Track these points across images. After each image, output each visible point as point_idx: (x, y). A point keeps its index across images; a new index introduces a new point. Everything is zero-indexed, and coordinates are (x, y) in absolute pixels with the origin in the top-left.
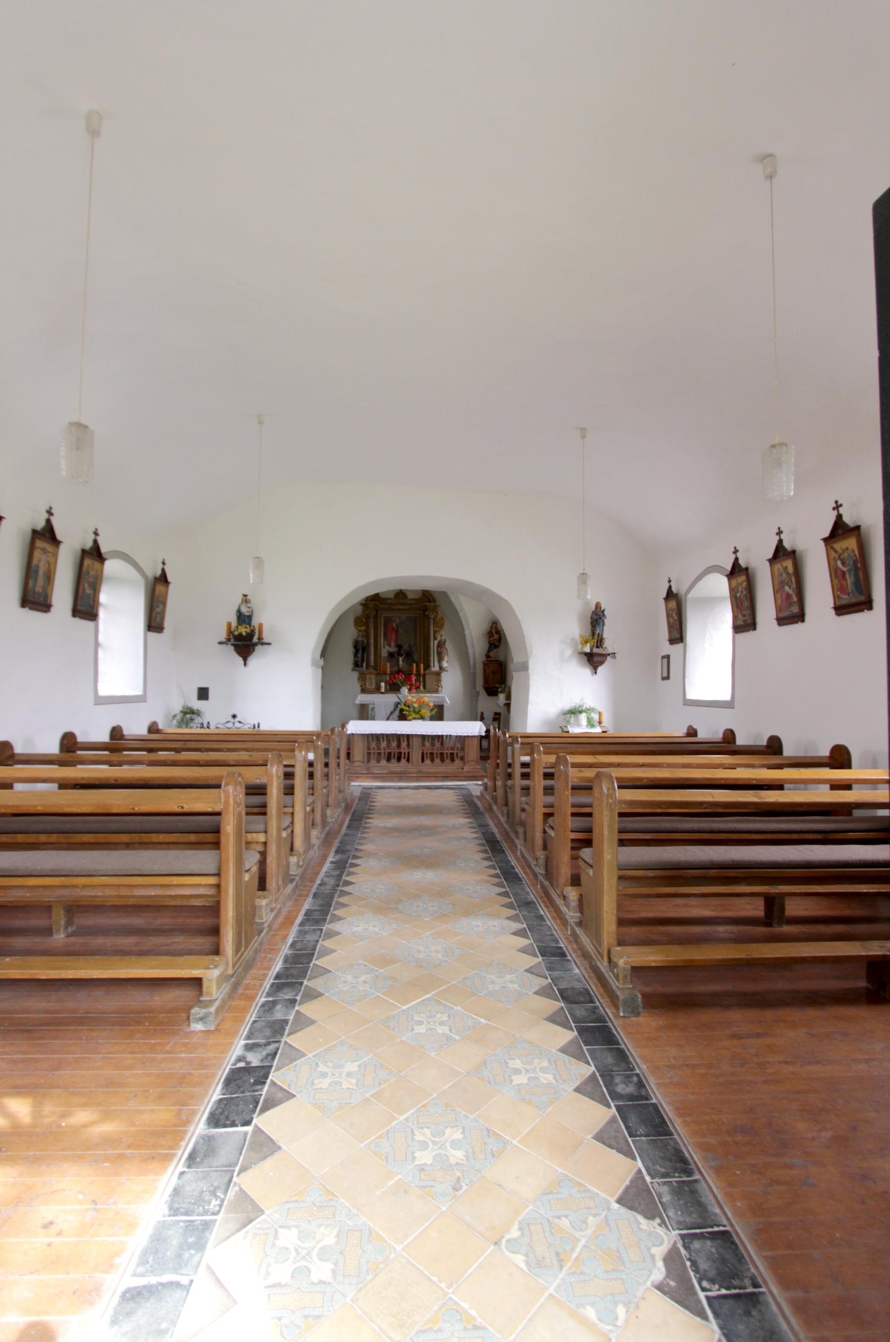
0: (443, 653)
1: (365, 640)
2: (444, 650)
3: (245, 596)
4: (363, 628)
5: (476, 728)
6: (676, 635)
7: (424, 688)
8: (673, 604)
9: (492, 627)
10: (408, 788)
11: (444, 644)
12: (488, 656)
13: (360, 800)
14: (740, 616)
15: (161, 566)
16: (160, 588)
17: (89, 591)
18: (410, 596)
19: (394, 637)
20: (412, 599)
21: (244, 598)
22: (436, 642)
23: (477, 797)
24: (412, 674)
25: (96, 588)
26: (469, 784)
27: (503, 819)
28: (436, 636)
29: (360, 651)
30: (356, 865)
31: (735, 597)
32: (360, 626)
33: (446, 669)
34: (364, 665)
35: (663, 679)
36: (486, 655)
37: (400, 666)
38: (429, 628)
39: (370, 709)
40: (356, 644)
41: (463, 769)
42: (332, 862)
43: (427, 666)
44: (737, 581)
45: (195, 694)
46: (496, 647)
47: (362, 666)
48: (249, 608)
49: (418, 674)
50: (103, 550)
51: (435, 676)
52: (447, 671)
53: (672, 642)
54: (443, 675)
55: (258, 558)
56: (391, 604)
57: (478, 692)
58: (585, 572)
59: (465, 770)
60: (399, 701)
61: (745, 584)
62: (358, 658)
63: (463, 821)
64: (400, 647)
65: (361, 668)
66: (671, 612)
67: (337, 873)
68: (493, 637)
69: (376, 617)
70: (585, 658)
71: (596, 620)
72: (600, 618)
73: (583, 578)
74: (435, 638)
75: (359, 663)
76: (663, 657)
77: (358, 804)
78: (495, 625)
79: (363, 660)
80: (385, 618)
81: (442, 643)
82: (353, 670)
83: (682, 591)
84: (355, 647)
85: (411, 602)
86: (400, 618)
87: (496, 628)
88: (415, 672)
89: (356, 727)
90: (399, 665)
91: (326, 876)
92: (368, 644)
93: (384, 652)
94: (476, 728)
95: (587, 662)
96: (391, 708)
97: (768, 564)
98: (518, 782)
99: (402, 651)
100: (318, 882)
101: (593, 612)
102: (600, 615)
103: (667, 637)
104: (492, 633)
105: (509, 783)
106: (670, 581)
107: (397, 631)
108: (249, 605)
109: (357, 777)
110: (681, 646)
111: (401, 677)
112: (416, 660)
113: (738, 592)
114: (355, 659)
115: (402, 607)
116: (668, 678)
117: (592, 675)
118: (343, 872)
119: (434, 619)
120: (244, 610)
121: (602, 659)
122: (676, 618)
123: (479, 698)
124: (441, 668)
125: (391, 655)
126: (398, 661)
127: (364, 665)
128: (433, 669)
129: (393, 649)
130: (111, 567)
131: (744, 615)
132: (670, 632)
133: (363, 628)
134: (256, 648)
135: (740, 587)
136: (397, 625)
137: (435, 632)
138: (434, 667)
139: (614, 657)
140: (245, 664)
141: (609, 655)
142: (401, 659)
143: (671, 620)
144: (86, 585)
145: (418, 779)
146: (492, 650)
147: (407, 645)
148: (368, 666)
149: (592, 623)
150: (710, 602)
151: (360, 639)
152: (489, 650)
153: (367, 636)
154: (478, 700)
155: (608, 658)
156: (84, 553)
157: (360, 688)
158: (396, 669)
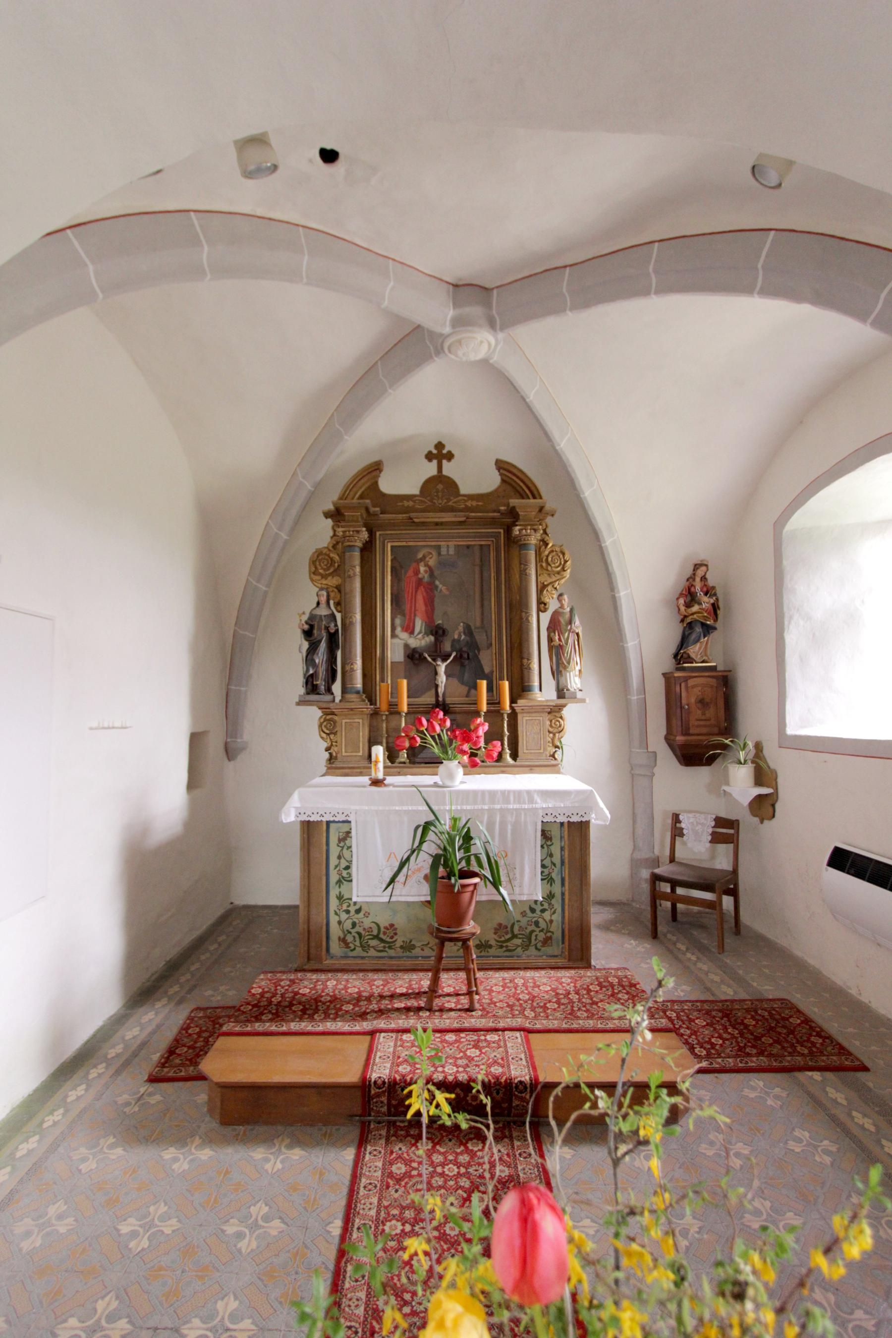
0: (569, 648)
1: (339, 616)
2: (572, 638)
4: (334, 581)
7: (515, 756)
9: (692, 578)
11: (570, 622)
12: (680, 657)
18: (463, 490)
19: (421, 604)
20: (471, 497)
22: (545, 618)
24: (477, 714)
28: (546, 600)
29: (323, 646)
32: (324, 577)
33: (579, 695)
34: (337, 688)
36: (675, 656)
37: (441, 690)
38: (524, 574)
40: (312, 627)
43: (520, 689)
46: (708, 629)
47: (329, 690)
49: (494, 713)
51: (545, 719)
52: (583, 701)
54: (570, 712)
56: (407, 510)
57: (655, 753)
60: (432, 818)
62: (314, 665)
64: (438, 632)
65: (328, 697)
68: (700, 604)
69: (368, 548)
74: (542, 606)
75: (321, 683)
79: (332, 675)
80: (392, 547)
81: (563, 620)
82: (301, 703)
84: (308, 634)
85: (469, 504)
86: (438, 548)
87: (704, 579)
88: (484, 707)
90: (437, 686)
92: (347, 626)
99: (447, 647)
107: (431, 588)
111: (442, 726)
112: (487, 670)
115: (448, 517)
119: (538, 553)
123: (656, 770)
125: (414, 657)
126: (436, 673)
129: (420, 640)
133: (334, 581)
137: (541, 589)
138: (541, 690)
142: (442, 667)
146: (697, 640)
147: (461, 627)
148: (344, 691)
151: (323, 611)
152: (684, 642)
154: (653, 775)
157: (327, 755)
158: (428, 699)
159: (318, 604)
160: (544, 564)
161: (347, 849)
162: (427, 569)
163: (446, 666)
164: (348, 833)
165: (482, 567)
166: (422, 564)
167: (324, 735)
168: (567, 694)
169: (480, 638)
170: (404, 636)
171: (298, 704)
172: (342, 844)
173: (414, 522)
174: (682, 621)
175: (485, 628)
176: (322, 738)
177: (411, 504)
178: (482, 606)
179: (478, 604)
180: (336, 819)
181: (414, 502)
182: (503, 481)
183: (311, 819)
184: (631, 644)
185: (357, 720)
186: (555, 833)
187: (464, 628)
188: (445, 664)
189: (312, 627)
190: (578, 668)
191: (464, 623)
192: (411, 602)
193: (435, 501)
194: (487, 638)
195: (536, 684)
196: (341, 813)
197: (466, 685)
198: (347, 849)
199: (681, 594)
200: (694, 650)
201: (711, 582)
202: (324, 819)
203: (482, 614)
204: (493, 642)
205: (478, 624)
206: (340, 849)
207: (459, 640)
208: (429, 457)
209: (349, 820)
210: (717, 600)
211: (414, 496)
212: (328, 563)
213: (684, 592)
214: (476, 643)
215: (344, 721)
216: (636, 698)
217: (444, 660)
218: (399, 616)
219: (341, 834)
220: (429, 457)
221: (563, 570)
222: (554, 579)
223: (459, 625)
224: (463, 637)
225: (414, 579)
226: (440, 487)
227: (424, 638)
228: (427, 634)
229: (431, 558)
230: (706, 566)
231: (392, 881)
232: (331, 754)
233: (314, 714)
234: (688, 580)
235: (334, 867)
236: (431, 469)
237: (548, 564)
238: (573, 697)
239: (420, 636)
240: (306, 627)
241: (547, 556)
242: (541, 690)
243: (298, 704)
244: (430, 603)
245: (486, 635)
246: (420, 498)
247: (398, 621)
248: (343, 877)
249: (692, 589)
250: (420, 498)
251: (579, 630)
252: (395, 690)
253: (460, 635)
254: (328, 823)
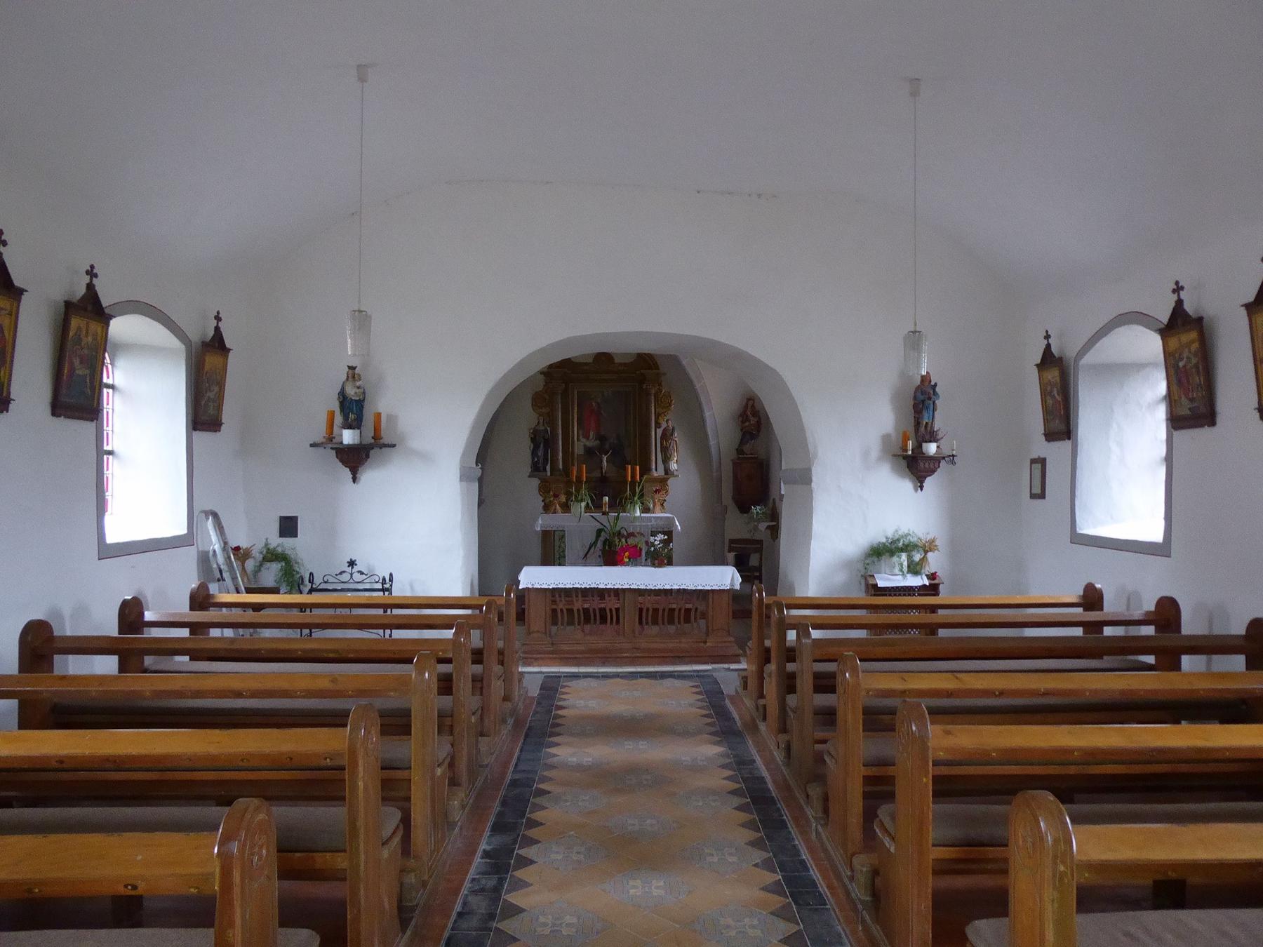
1: (549, 429)
3: (352, 368)
5: (724, 577)
6: (1058, 425)
8: (1053, 375)
9: (747, 404)
10: (617, 675)
12: (740, 451)
13: (539, 703)
14: (1184, 401)
15: (214, 323)
16: (211, 360)
17: (81, 371)
18: (617, 360)
20: (621, 364)
21: (351, 372)
22: (660, 431)
23: (732, 698)
25: (95, 366)
26: (714, 670)
27: (779, 756)
30: (527, 862)
31: (1176, 367)
33: (676, 473)
34: (548, 468)
35: (1033, 496)
38: (648, 410)
39: (557, 538)
40: (535, 436)
41: (705, 642)
42: (486, 854)
43: (646, 469)
44: (1180, 340)
45: (275, 527)
47: (545, 470)
48: (359, 388)
50: (105, 302)
53: (1050, 436)
55: (360, 311)
58: (918, 330)
59: (708, 644)
60: (602, 527)
61: (1195, 346)
63: (710, 750)
64: (602, 439)
65: (544, 473)
66: (1049, 388)
67: (491, 882)
68: (749, 421)
70: (904, 463)
71: (923, 401)
72: (930, 398)
73: (914, 339)
74: (658, 425)
76: (1033, 461)
77: (536, 713)
78: (750, 403)
83: (1070, 353)
84: (533, 440)
87: (753, 406)
89: (534, 577)
90: (602, 468)
91: (474, 892)
93: (579, 449)
94: (724, 577)
95: (907, 470)
96: (592, 538)
97: (1243, 312)
98: (807, 699)
99: (607, 446)
100: (458, 908)
101: (918, 388)
102: (929, 393)
103: (1040, 428)
104: (747, 416)
105: (792, 700)
106: (1047, 337)
108: (358, 384)
109: (536, 659)
110: (1065, 445)
113: (1181, 359)
114: (533, 459)
116: (1042, 495)
117: (916, 490)
118: (501, 881)
120: (351, 391)
121: (932, 466)
122: (1059, 398)
124: (667, 471)
125: (589, 452)
126: (602, 461)
127: (548, 468)
128: (655, 474)
130: (119, 327)
131: (1192, 400)
132: (1046, 421)
134: (372, 452)
135: (1187, 350)
138: (656, 470)
139: (953, 463)
140: (354, 480)
141: (944, 458)
143: (1050, 402)
144: (77, 362)
145: (633, 661)
148: (552, 469)
149: (915, 406)
150: (1122, 371)
151: (542, 428)
152: (742, 442)
153: (552, 422)
154: (725, 519)
155: (943, 463)
156: (69, 308)
157: (543, 504)
158: (597, 474)
159: (538, 423)
160: (660, 402)
164: (563, 536)
168: (669, 473)
170: (584, 440)
171: (529, 476)
174: (742, 430)
184: (712, 442)
189: (535, 436)
190: (675, 459)
195: (654, 467)
199: (741, 415)
200: (747, 448)
210: (760, 418)
211: (590, 363)
221: (670, 405)
222: (665, 410)
228: (596, 440)
230: (754, 400)
231: (586, 555)
232: (545, 504)
233: (535, 482)
237: (661, 402)
238: (672, 474)
241: (662, 398)
242: (656, 470)
243: (529, 476)
247: (581, 432)
251: (677, 439)
252: (579, 471)
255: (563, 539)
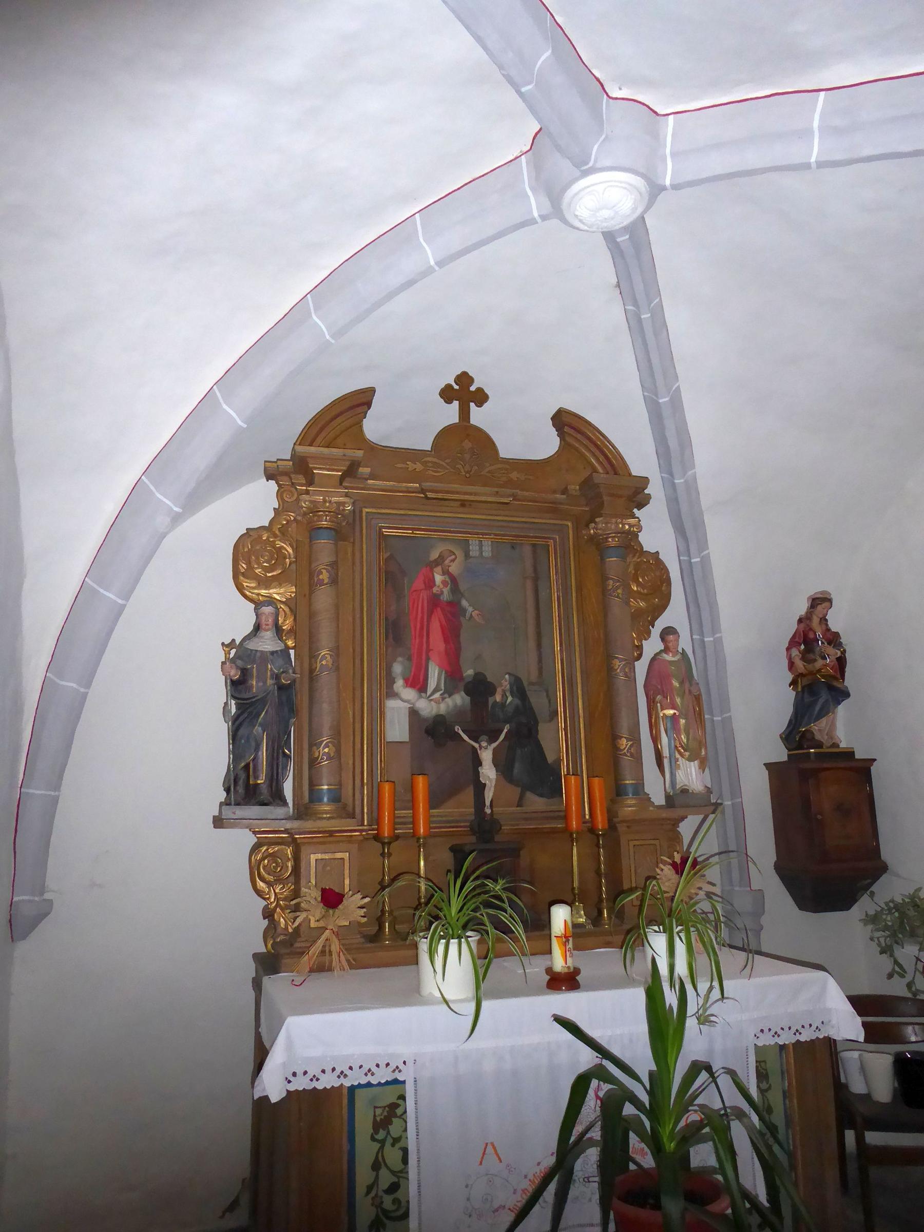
19: (437, 642)
32: (265, 583)
37: (489, 795)
40: (245, 672)
47: (277, 797)
56: (414, 477)
84: (237, 686)
85: (514, 475)
87: (824, 620)
90: (480, 788)
107: (453, 611)
126: (478, 763)
136: (453, 581)
142: (486, 756)
147: (506, 683)
151: (267, 643)
159: (257, 628)
161: (393, 1145)
162: (447, 579)
163: (494, 749)
165: (536, 580)
166: (438, 569)
167: (261, 885)
169: (537, 701)
170: (409, 694)
171: (218, 822)
172: (381, 1135)
173: (427, 498)
175: (545, 684)
176: (259, 893)
177: (419, 467)
178: (539, 645)
179: (532, 644)
180: (374, 1081)
181: (425, 464)
182: (565, 445)
183: (320, 1086)
185: (339, 855)
186: (773, 1065)
187: (510, 684)
188: (494, 745)
191: (510, 674)
192: (421, 636)
193: (459, 466)
194: (550, 701)
196: (382, 1065)
197: (517, 785)
198: (393, 1145)
199: (793, 643)
201: (834, 626)
202: (347, 1083)
203: (540, 661)
204: (560, 709)
205: (534, 676)
206: (377, 1146)
207: (503, 705)
208: (447, 394)
209: (401, 1079)
212: (272, 558)
213: (797, 639)
214: (531, 708)
215: (313, 857)
216: (730, 803)
217: (492, 740)
218: (400, 659)
219: (378, 1111)
220: (447, 394)
223: (504, 677)
224: (510, 699)
225: (424, 595)
226: (467, 444)
227: (443, 699)
228: (449, 692)
229: (453, 561)
234: (800, 621)
235: (364, 1190)
236: (450, 414)
239: (437, 695)
240: (235, 674)
244: (452, 634)
245: (548, 696)
246: (435, 460)
248: (385, 1212)
249: (811, 636)
250: (435, 460)
253: (504, 696)
254: (352, 1089)
255: (395, 1128)
